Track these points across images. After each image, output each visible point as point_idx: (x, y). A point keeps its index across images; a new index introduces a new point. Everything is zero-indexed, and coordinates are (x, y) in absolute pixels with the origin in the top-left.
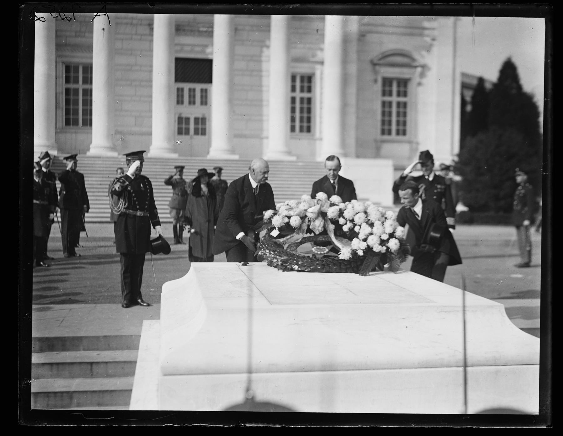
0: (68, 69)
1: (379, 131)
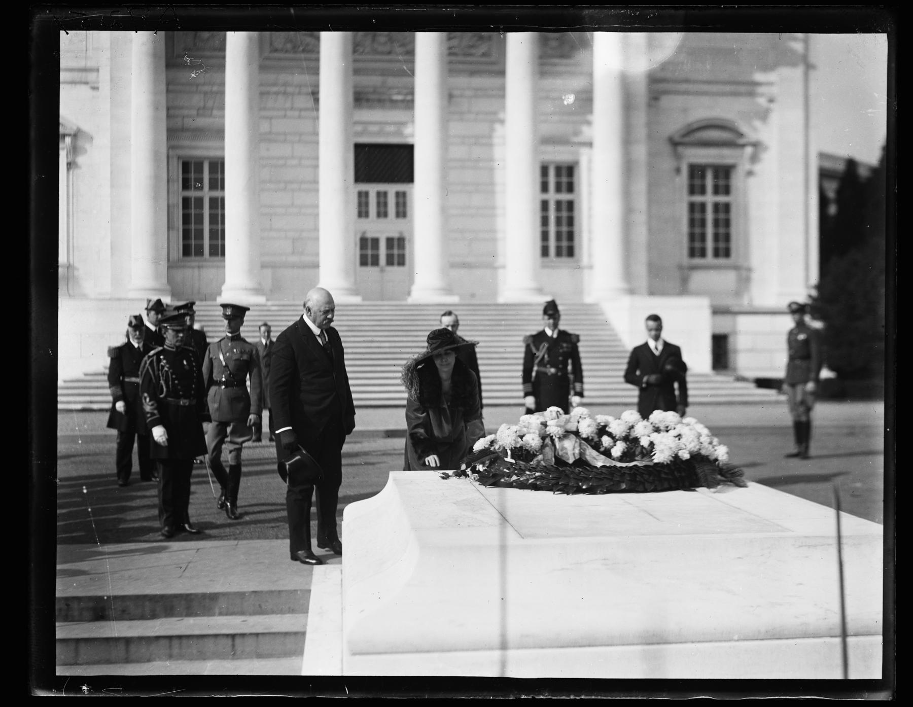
0: (186, 166)
1: (685, 251)
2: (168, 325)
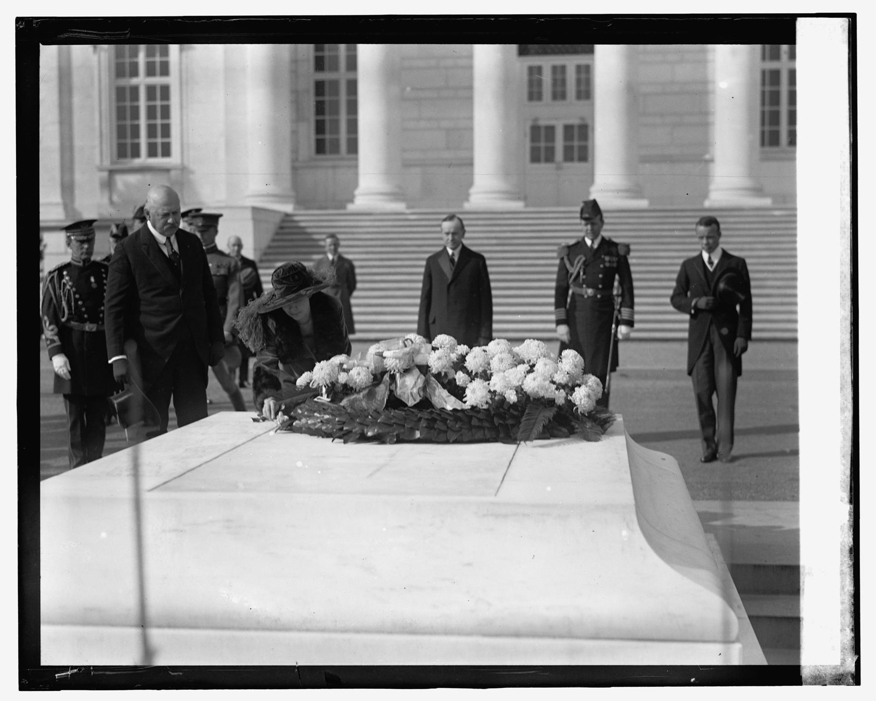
2: (71, 234)
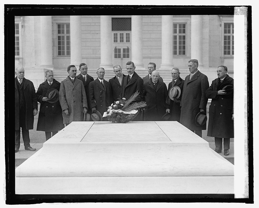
0: (59, 26)
1: (223, 52)
